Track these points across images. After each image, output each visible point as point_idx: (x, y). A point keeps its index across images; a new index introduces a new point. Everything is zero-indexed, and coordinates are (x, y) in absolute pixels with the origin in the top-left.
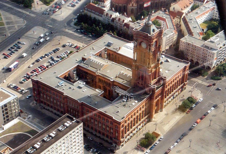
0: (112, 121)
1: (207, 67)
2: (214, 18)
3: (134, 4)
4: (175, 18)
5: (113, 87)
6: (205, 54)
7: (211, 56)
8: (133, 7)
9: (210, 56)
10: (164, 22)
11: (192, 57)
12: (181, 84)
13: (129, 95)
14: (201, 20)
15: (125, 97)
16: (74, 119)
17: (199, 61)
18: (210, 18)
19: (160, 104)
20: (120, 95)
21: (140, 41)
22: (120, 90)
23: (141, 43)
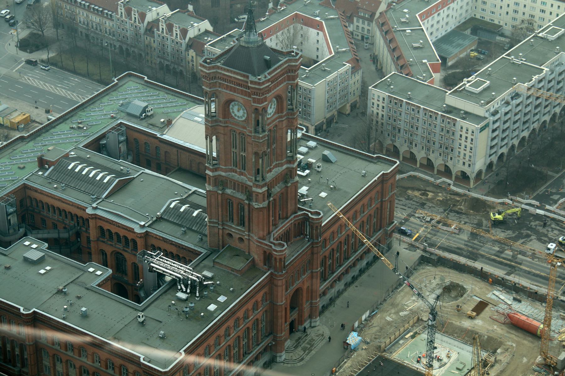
0: (138, 369)
1: (459, 174)
2: (478, 16)
4: (355, 19)
5: (144, 254)
6: (448, 132)
7: (466, 138)
9: (463, 138)
10: (318, 33)
11: (411, 143)
12: (375, 231)
13: (198, 277)
14: (438, 22)
15: (186, 287)
17: (432, 157)
18: (464, 15)
19: (304, 299)
20: (168, 279)
21: (223, 99)
22: (169, 262)
23: (231, 102)
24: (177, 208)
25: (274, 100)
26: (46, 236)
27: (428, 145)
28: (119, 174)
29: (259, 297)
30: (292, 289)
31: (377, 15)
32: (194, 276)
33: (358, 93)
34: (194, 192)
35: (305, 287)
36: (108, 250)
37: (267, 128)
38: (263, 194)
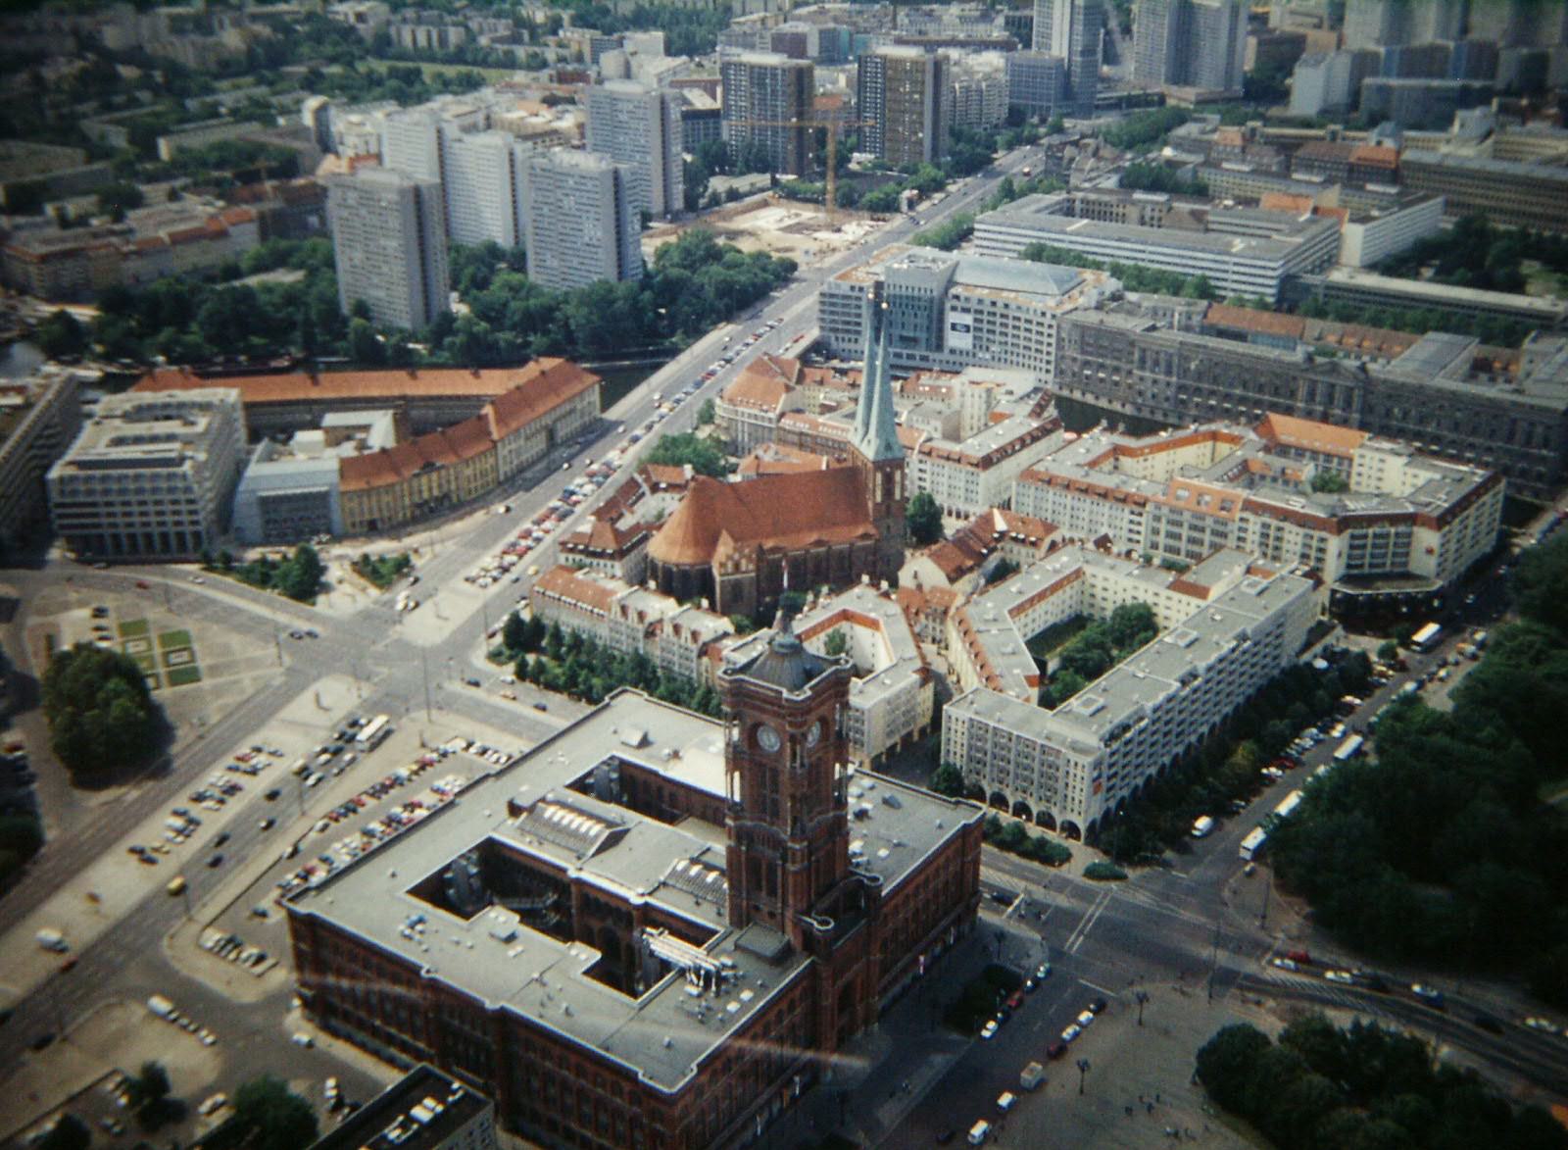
3: (744, 562)
5: (643, 932)
8: (738, 576)
14: (1034, 620)
15: (699, 978)
16: (456, 1085)
18: (1068, 611)
19: (858, 997)
21: (749, 722)
24: (686, 870)
25: (818, 724)
26: (515, 906)
27: (1025, 785)
28: (609, 824)
29: (797, 993)
30: (840, 983)
31: (952, 611)
32: (709, 964)
33: (929, 713)
34: (708, 850)
35: (859, 980)
36: (596, 925)
37: (806, 761)
38: (801, 850)
